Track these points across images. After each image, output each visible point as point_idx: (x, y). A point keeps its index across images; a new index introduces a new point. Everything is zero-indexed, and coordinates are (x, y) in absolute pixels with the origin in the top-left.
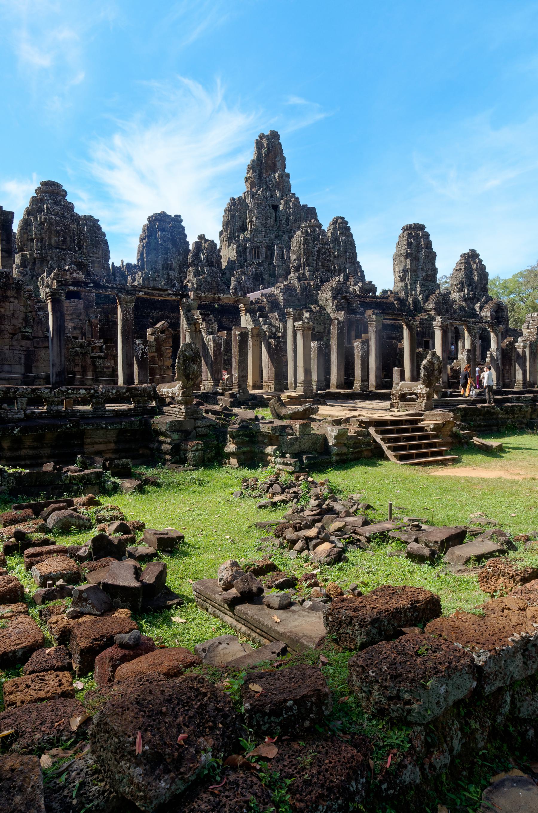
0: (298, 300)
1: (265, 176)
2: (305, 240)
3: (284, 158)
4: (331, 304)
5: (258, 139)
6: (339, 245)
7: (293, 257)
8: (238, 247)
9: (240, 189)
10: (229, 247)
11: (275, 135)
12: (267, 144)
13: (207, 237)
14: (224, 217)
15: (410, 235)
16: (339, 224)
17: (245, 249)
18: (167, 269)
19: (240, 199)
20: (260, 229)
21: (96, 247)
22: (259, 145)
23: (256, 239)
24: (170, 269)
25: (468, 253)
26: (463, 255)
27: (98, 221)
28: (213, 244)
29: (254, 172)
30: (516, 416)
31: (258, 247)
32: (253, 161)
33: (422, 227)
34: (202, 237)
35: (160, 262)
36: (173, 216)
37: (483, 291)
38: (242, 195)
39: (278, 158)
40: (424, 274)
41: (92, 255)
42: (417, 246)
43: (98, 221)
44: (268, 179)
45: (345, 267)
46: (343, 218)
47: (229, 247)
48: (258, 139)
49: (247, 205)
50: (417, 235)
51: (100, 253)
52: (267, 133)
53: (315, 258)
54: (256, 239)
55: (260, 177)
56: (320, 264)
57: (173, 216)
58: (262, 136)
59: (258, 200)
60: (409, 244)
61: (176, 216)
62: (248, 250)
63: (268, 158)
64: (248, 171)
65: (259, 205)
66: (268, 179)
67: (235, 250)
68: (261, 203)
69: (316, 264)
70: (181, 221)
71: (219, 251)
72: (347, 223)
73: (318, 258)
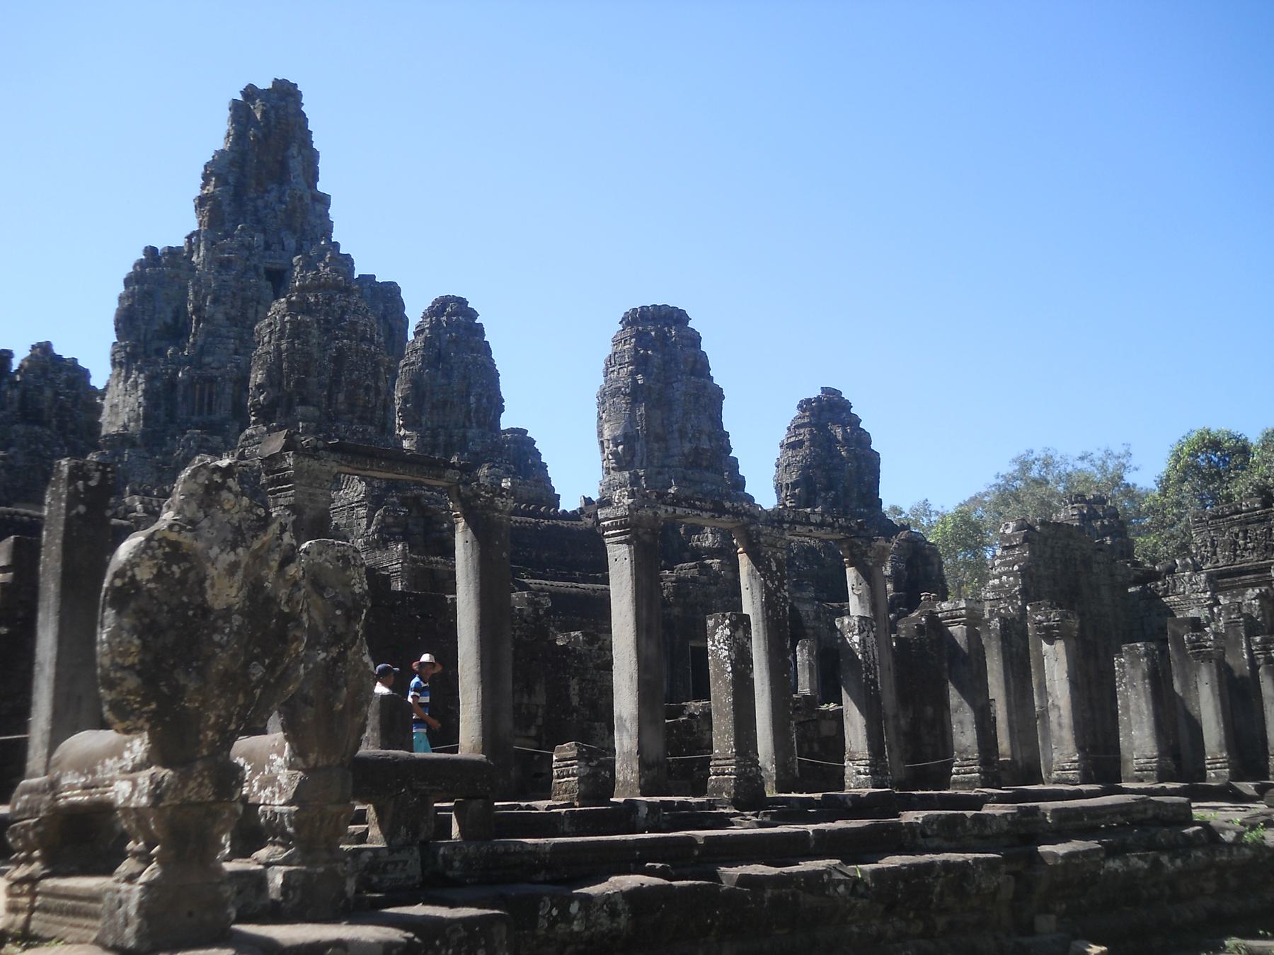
1: (252, 195)
2: (296, 326)
3: (314, 155)
4: (364, 522)
5: (240, 98)
7: (257, 377)
8: (149, 380)
10: (127, 378)
12: (264, 113)
14: (121, 298)
15: (641, 338)
16: (449, 316)
17: (172, 384)
19: (172, 252)
20: (224, 331)
22: (240, 112)
23: (208, 359)
25: (818, 399)
26: (805, 405)
28: (76, 374)
29: (222, 181)
30: (941, 922)
31: (212, 380)
32: (220, 154)
33: (676, 317)
37: (867, 506)
38: (180, 242)
39: (294, 150)
40: (687, 447)
42: (663, 370)
44: (260, 203)
45: (464, 436)
46: (462, 302)
47: (127, 378)
48: (240, 98)
49: (192, 268)
50: (664, 338)
52: (265, 84)
53: (325, 379)
54: (208, 359)
55: (238, 195)
56: (341, 397)
58: (250, 92)
59: (223, 251)
60: (640, 363)
62: (181, 388)
63: (267, 153)
64: (206, 178)
65: (225, 265)
66: (260, 203)
67: (142, 387)
68: (229, 260)
69: (330, 397)
71: (102, 394)
72: (473, 314)
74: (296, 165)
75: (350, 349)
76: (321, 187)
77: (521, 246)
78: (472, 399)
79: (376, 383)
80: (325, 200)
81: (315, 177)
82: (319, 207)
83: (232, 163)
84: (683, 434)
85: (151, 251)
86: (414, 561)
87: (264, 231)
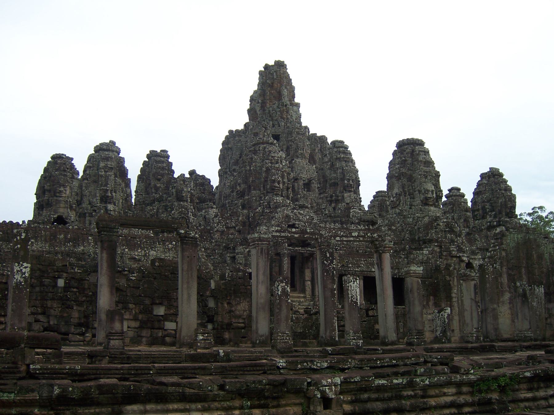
0: (239, 231)
1: (268, 106)
5: (263, 70)
6: (335, 172)
9: (239, 120)
11: (280, 65)
13: (198, 172)
18: (106, 203)
21: (64, 186)
24: (110, 203)
27: (72, 159)
32: (255, 92)
33: (419, 143)
34: (192, 173)
35: (98, 195)
36: (159, 151)
41: (58, 195)
43: (72, 159)
44: (271, 109)
51: (68, 192)
56: (268, 187)
57: (159, 151)
61: (161, 151)
70: (168, 157)
73: (266, 181)
74: (285, 92)
75: (271, 167)
76: (296, 100)
77: (358, 120)
78: (346, 182)
79: (283, 180)
80: (298, 105)
81: (294, 97)
82: (295, 108)
83: (260, 95)
84: (420, 192)
85: (231, 132)
86: (289, 249)
87: (272, 120)
